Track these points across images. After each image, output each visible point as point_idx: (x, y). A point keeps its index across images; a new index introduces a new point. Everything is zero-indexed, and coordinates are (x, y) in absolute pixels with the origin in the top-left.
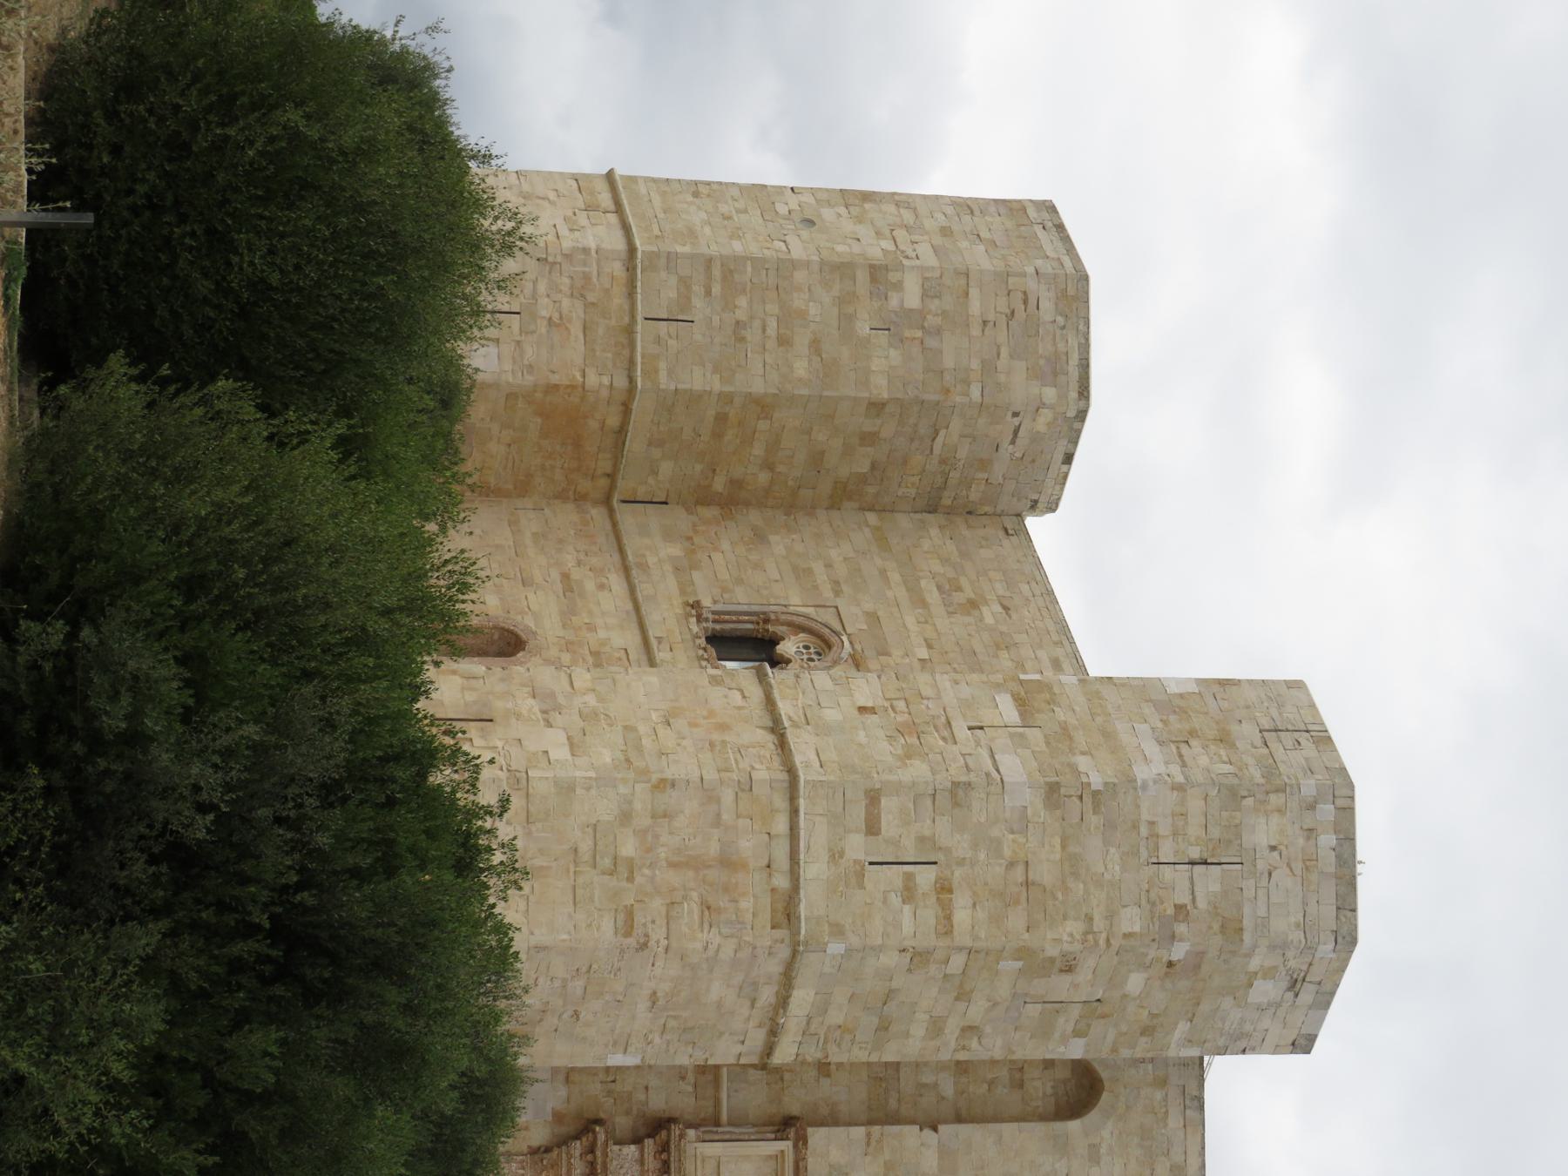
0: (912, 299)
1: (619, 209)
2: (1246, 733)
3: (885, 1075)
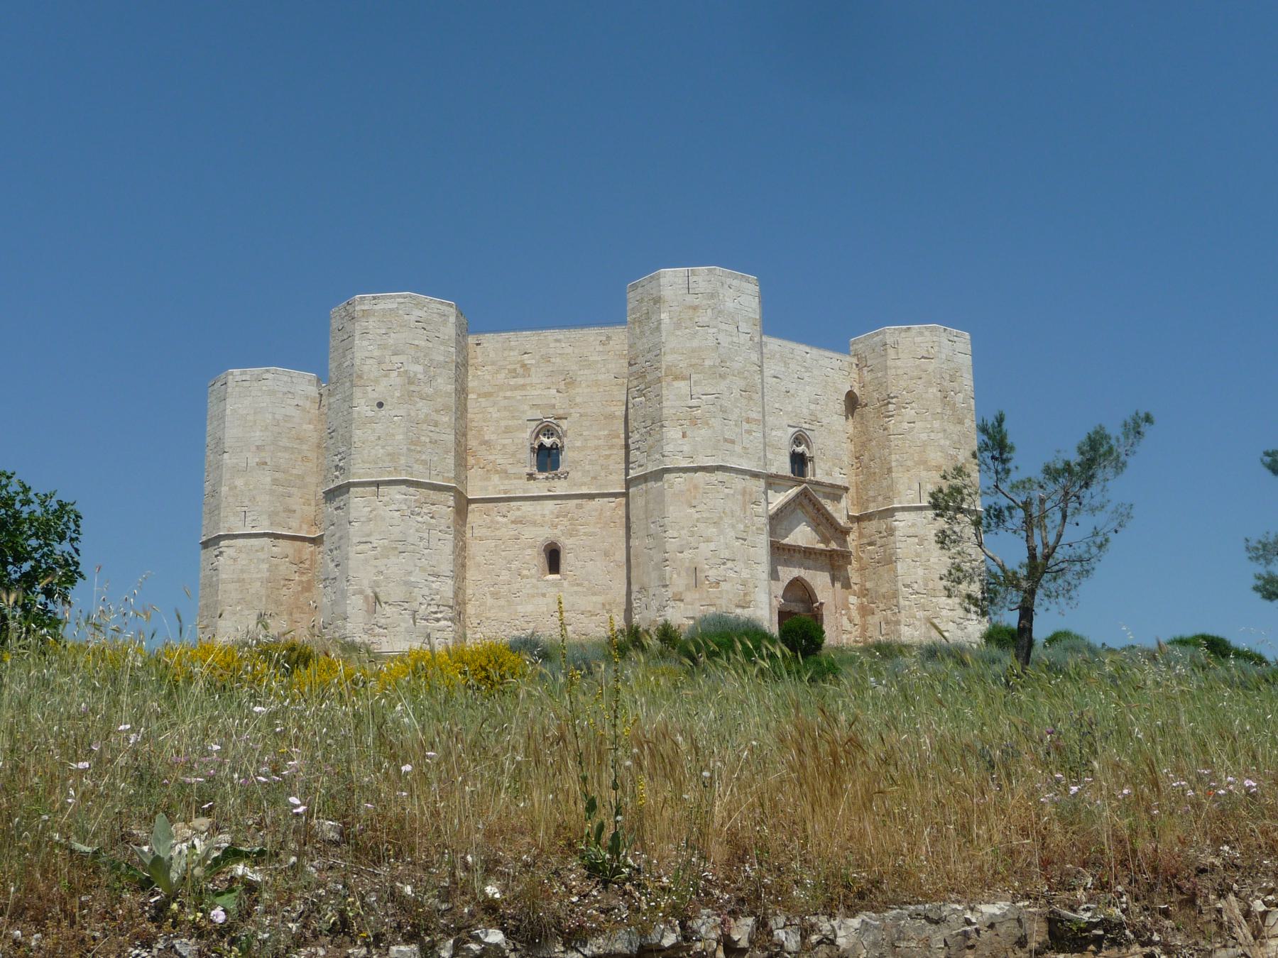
0: (419, 368)
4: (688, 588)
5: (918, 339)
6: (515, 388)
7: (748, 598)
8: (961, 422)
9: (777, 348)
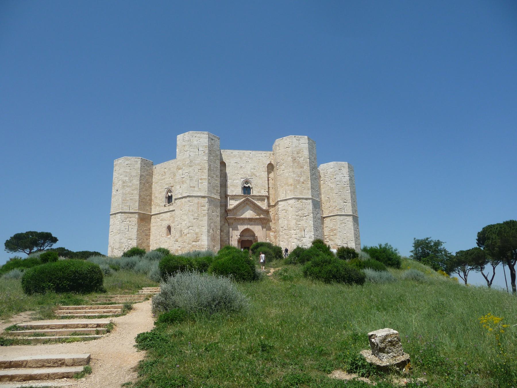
0: (127, 178)
1: (115, 214)
2: (184, 143)
3: (221, 186)
4: (179, 237)
5: (285, 142)
6: (162, 180)
7: (198, 239)
8: (302, 167)
9: (237, 153)
